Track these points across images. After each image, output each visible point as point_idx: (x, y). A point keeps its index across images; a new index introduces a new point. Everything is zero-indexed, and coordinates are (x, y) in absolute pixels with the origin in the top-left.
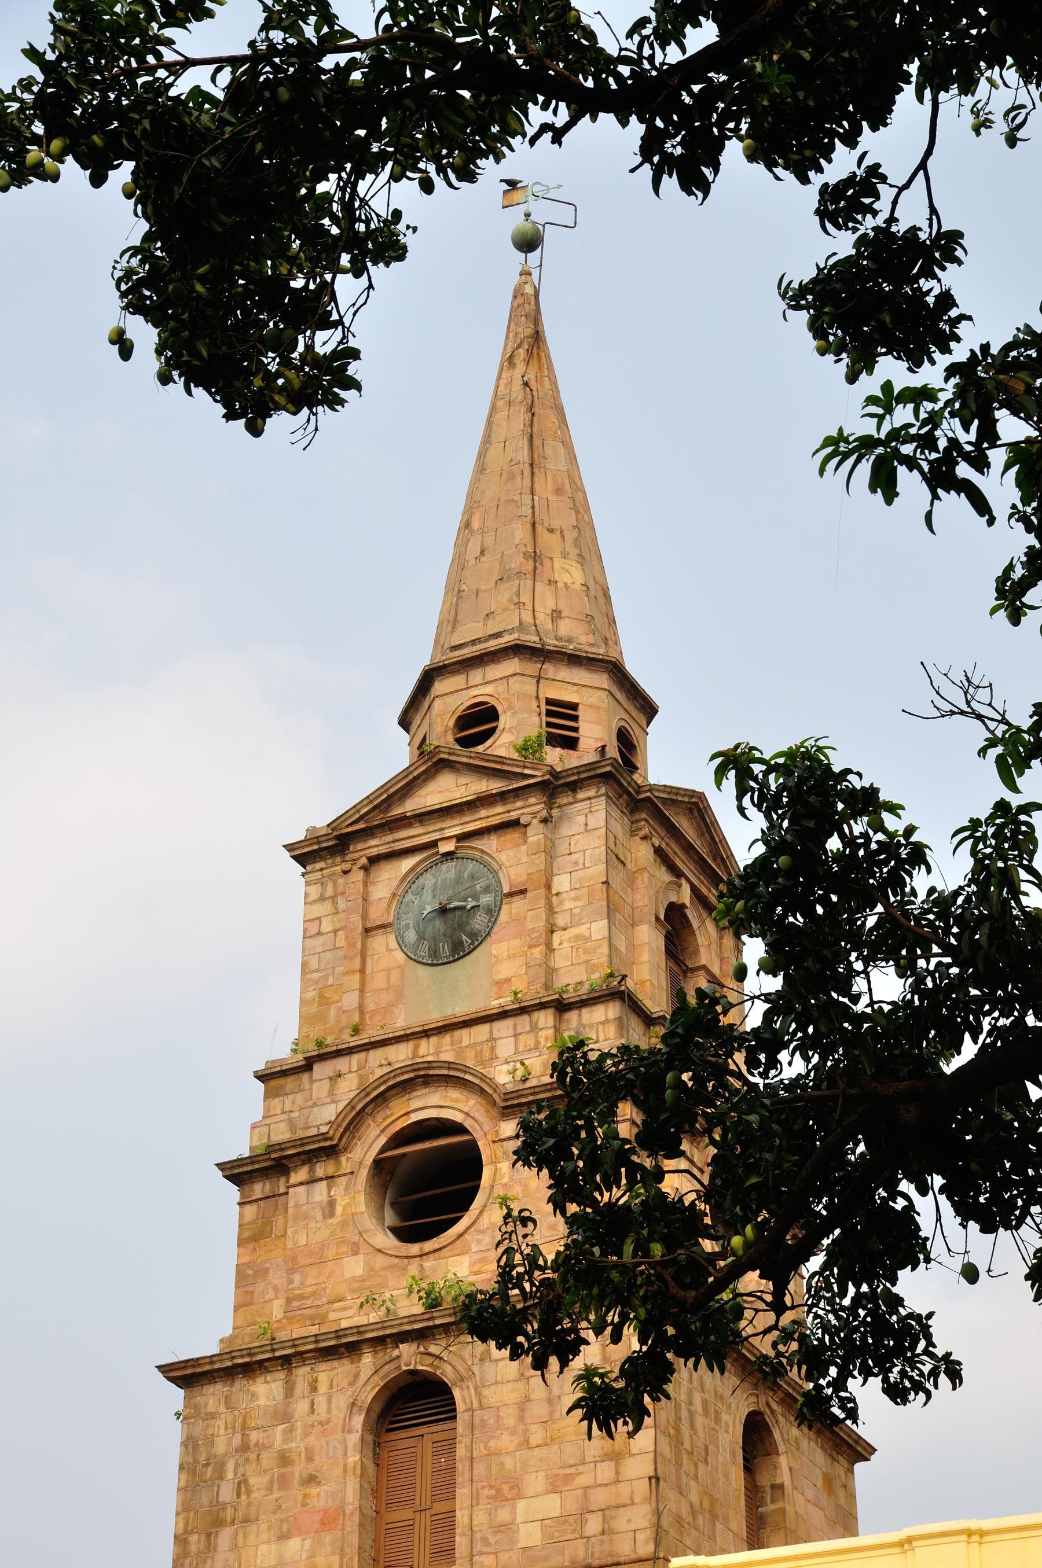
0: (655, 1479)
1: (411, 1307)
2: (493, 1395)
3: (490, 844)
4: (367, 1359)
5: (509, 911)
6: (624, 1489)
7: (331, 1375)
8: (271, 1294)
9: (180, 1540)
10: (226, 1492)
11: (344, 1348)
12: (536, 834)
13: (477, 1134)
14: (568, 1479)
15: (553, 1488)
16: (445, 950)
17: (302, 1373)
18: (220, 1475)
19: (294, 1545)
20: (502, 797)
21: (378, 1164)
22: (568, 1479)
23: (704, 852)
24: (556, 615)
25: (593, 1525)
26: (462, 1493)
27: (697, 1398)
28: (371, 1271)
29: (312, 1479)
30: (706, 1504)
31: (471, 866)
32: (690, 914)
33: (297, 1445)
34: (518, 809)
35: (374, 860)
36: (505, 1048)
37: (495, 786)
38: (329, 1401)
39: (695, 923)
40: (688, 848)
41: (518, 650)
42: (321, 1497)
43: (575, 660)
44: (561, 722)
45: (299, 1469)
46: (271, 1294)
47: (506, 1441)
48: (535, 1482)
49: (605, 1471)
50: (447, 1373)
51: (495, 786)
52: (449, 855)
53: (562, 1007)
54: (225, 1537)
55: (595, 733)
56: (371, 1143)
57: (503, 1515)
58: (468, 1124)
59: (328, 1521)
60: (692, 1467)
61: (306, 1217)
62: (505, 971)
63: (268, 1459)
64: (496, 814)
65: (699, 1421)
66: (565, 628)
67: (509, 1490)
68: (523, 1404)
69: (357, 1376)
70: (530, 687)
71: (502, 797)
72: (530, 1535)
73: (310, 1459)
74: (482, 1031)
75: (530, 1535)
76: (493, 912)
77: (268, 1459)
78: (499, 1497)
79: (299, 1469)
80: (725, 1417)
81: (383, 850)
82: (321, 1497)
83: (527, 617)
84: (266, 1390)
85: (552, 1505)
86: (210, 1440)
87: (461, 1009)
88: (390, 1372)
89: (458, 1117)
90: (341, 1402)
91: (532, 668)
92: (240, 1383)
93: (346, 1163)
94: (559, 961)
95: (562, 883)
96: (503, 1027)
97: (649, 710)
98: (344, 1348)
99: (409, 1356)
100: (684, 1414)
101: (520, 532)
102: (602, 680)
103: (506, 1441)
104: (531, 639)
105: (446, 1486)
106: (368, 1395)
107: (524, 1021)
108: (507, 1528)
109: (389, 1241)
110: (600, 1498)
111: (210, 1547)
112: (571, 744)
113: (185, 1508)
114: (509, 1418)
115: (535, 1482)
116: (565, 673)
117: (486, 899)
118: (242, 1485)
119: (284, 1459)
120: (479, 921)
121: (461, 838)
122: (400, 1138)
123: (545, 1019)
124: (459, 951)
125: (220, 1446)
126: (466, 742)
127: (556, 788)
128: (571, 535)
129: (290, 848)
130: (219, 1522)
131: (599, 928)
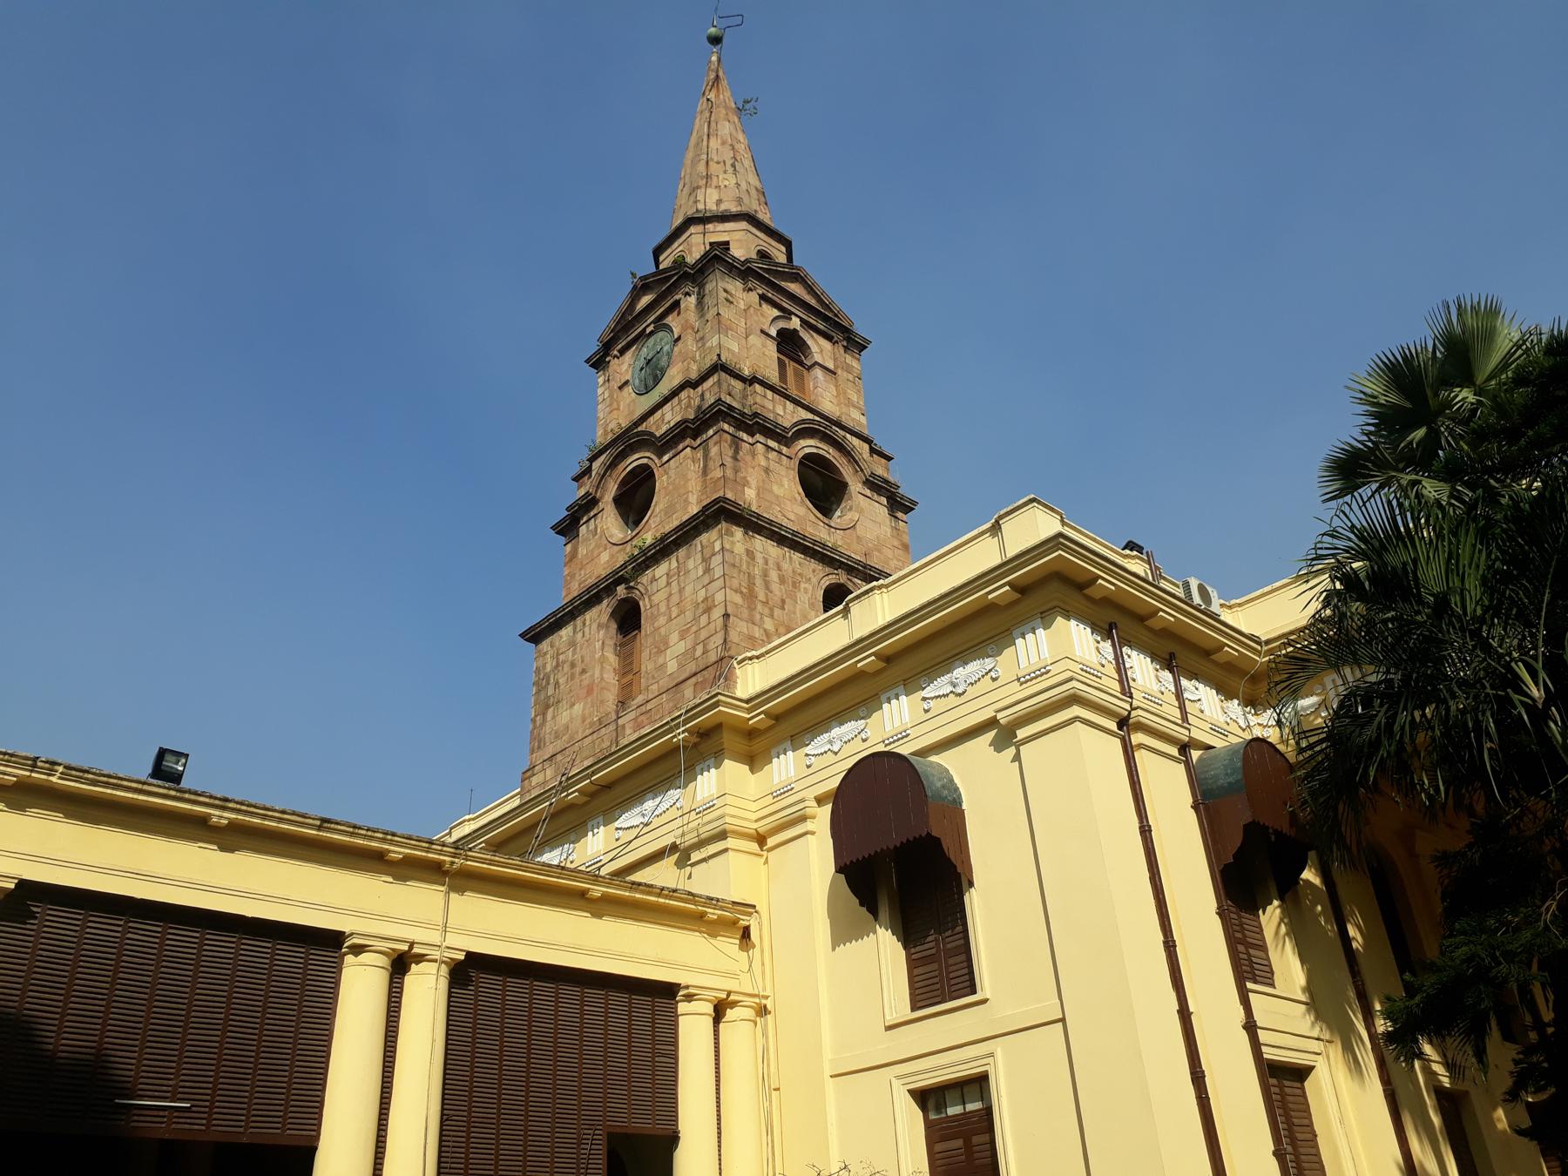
0: (726, 616)
3: (669, 320)
6: (712, 626)
7: (590, 615)
11: (590, 599)
15: (682, 638)
16: (651, 383)
19: (578, 708)
21: (618, 501)
23: (813, 302)
24: (719, 202)
27: (774, 575)
28: (612, 556)
29: (584, 671)
30: (782, 630)
32: (804, 335)
35: (622, 352)
36: (668, 417)
39: (810, 342)
40: (792, 297)
45: (578, 670)
48: (674, 637)
49: (704, 620)
52: (652, 333)
56: (612, 489)
57: (661, 660)
60: (767, 611)
63: (566, 667)
65: (775, 587)
66: (723, 207)
67: (662, 647)
70: (699, 238)
72: (672, 666)
74: (658, 414)
76: (669, 354)
77: (566, 667)
78: (660, 652)
79: (578, 670)
80: (803, 585)
83: (701, 206)
84: (565, 633)
85: (681, 647)
86: (544, 666)
88: (614, 602)
90: (594, 626)
91: (700, 228)
96: (667, 407)
98: (590, 599)
100: (759, 581)
101: (701, 168)
102: (744, 225)
103: (662, 620)
107: (676, 400)
108: (664, 665)
111: (544, 720)
114: (663, 608)
115: (674, 637)
116: (721, 227)
117: (666, 348)
118: (557, 683)
120: (663, 363)
122: (623, 483)
124: (657, 381)
125: (548, 668)
128: (729, 163)
129: (587, 361)
130: (547, 707)
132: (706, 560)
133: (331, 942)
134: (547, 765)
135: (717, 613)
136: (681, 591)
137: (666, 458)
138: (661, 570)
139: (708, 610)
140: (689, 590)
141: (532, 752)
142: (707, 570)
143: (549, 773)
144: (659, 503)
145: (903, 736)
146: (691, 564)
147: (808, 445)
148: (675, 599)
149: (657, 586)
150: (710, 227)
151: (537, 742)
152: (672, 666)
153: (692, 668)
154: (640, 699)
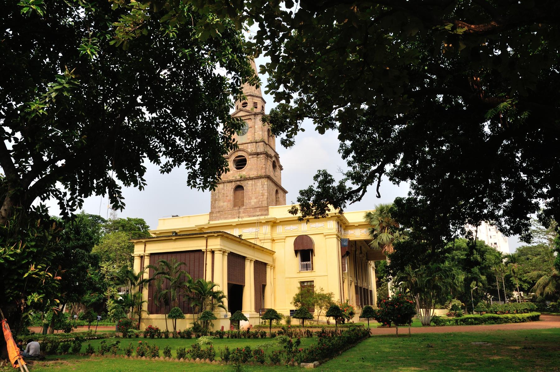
1: (238, 178)
2: (248, 188)
5: (250, 130)
9: (212, 202)
10: (217, 197)
11: (231, 182)
12: (253, 120)
17: (225, 184)
20: (249, 115)
21: (234, 160)
25: (260, 203)
26: (245, 199)
33: (225, 192)
34: (251, 117)
36: (249, 147)
37: (248, 114)
41: (250, 95)
42: (228, 198)
43: (257, 97)
44: (255, 105)
45: (225, 195)
47: (250, 193)
49: (262, 197)
50: (243, 185)
51: (248, 114)
53: (256, 142)
54: (217, 202)
55: (259, 106)
59: (229, 201)
62: (249, 137)
64: (248, 117)
67: (250, 198)
68: (252, 189)
71: (249, 115)
75: (253, 203)
76: (247, 130)
79: (225, 195)
82: (228, 198)
85: (255, 200)
87: (244, 142)
88: (236, 185)
90: (230, 188)
91: (252, 98)
94: (256, 136)
95: (256, 127)
97: (265, 103)
98: (231, 182)
99: (238, 183)
102: (260, 99)
103: (250, 193)
104: (252, 94)
105: (243, 197)
106: (234, 187)
108: (250, 203)
109: (235, 169)
110: (261, 200)
111: (215, 203)
112: (256, 108)
113: (212, 199)
114: (250, 190)
115: (253, 198)
118: (219, 196)
119: (224, 194)
120: (246, 131)
122: (237, 157)
123: (254, 144)
126: (243, 107)
127: (256, 114)
130: (216, 200)
131: (261, 133)
132: (263, 185)
133: (244, 258)
135: (265, 197)
136: (255, 189)
137: (250, 157)
138: (250, 182)
139: (263, 195)
140: (257, 189)
141: (211, 208)
142: (263, 187)
144: (247, 167)
145: (306, 232)
146: (258, 184)
147: (274, 159)
148: (254, 190)
149: (248, 185)
150: (254, 98)
151: (213, 206)
152: (253, 203)
153: (258, 205)
154: (244, 207)
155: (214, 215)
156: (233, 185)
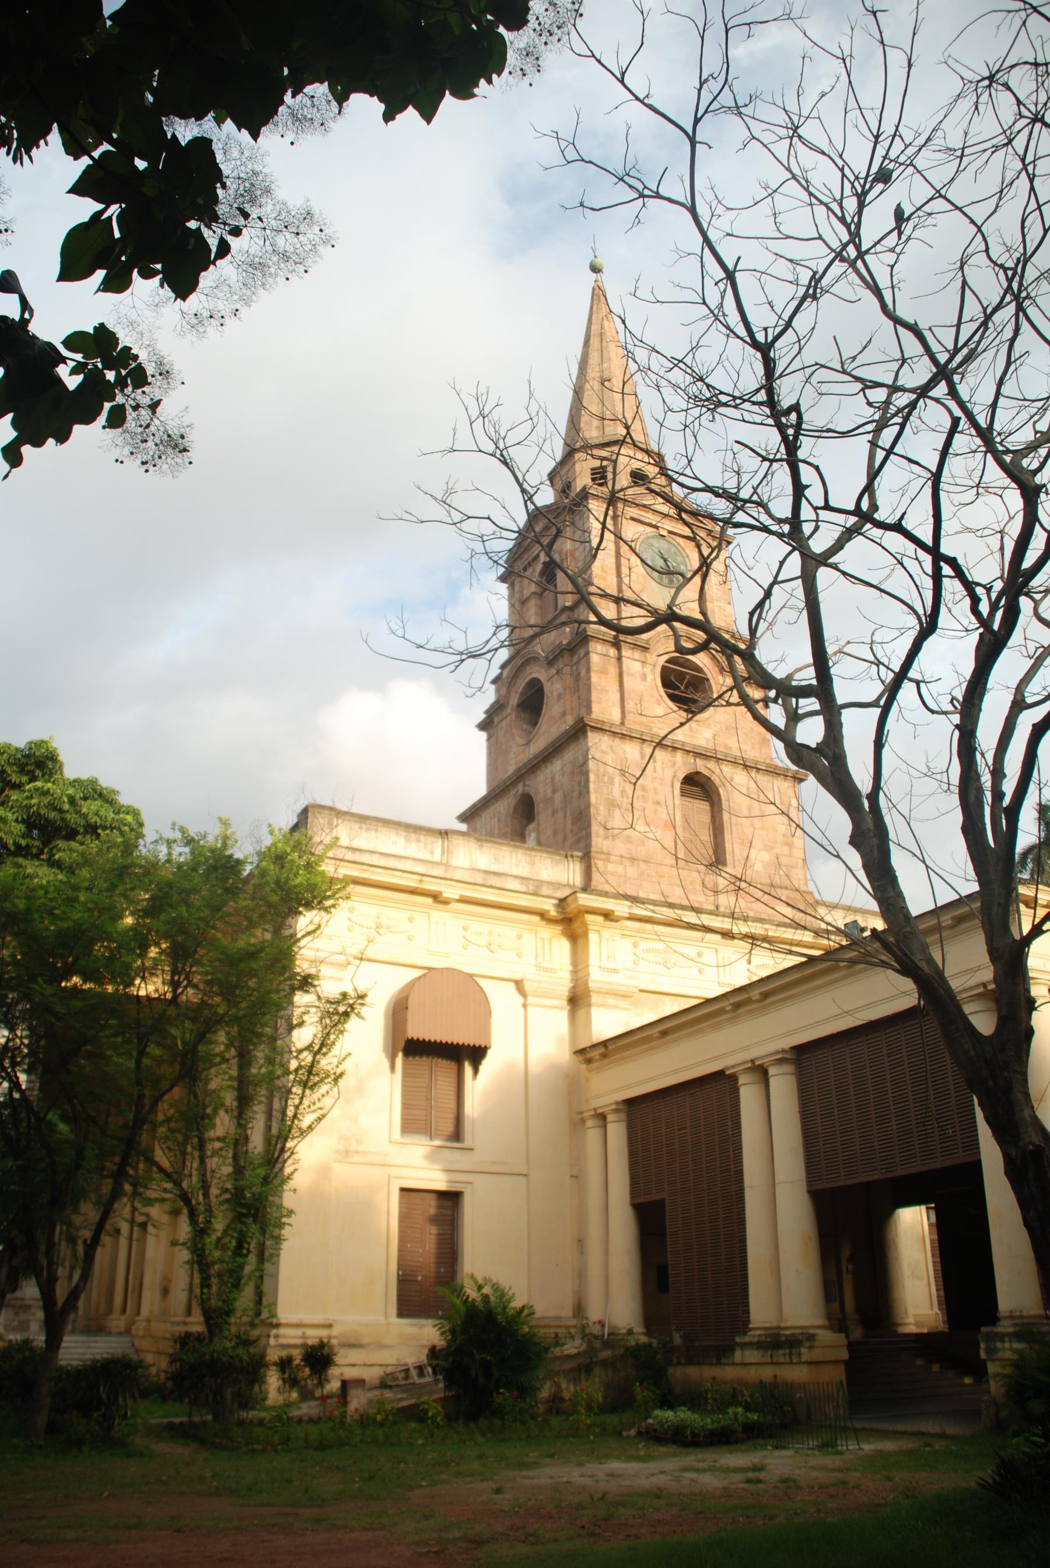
4: (679, 756)
8: (610, 704)
13: (710, 676)
14: (772, 848)
18: (611, 781)
22: (772, 848)
31: (673, 549)
38: (663, 769)
46: (610, 704)
58: (705, 669)
61: (632, 675)
69: (675, 764)
73: (656, 793)
81: (635, 516)
89: (701, 665)
90: (668, 774)
92: (617, 741)
93: (651, 658)
99: (701, 766)
121: (670, 532)
134: (627, 863)
138: (740, 778)
143: (631, 871)
155: (611, 867)
156: (682, 765)
